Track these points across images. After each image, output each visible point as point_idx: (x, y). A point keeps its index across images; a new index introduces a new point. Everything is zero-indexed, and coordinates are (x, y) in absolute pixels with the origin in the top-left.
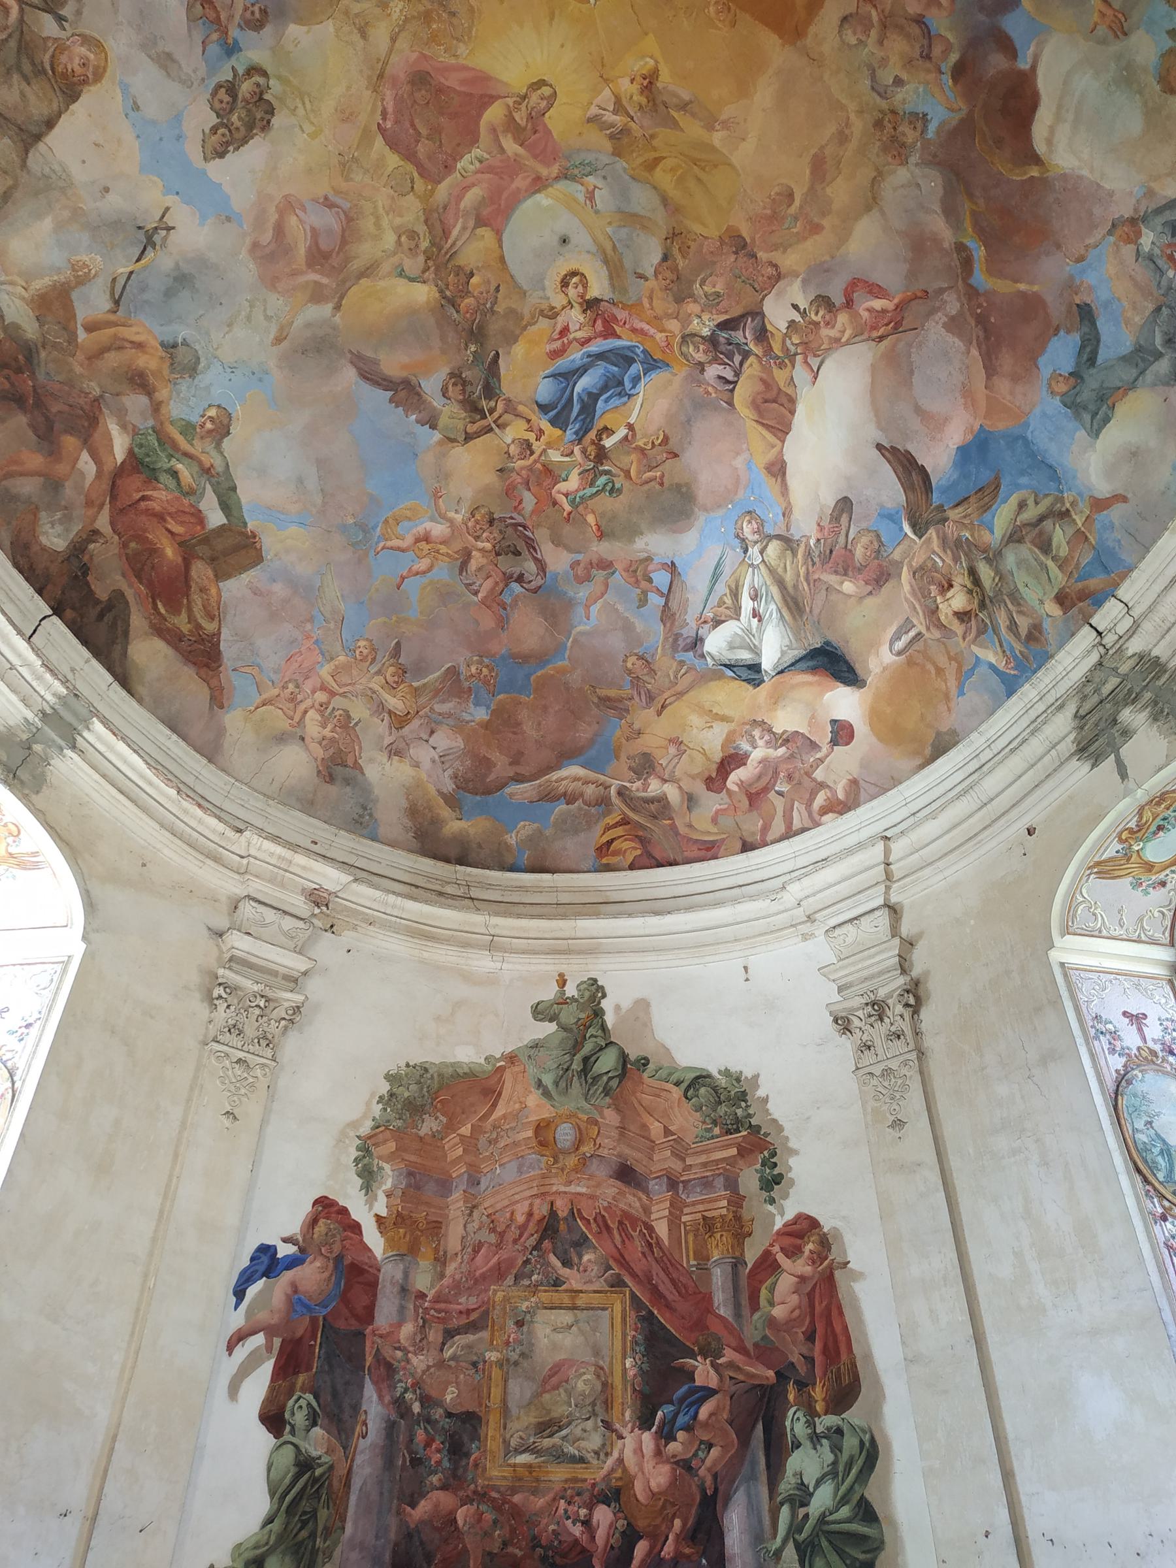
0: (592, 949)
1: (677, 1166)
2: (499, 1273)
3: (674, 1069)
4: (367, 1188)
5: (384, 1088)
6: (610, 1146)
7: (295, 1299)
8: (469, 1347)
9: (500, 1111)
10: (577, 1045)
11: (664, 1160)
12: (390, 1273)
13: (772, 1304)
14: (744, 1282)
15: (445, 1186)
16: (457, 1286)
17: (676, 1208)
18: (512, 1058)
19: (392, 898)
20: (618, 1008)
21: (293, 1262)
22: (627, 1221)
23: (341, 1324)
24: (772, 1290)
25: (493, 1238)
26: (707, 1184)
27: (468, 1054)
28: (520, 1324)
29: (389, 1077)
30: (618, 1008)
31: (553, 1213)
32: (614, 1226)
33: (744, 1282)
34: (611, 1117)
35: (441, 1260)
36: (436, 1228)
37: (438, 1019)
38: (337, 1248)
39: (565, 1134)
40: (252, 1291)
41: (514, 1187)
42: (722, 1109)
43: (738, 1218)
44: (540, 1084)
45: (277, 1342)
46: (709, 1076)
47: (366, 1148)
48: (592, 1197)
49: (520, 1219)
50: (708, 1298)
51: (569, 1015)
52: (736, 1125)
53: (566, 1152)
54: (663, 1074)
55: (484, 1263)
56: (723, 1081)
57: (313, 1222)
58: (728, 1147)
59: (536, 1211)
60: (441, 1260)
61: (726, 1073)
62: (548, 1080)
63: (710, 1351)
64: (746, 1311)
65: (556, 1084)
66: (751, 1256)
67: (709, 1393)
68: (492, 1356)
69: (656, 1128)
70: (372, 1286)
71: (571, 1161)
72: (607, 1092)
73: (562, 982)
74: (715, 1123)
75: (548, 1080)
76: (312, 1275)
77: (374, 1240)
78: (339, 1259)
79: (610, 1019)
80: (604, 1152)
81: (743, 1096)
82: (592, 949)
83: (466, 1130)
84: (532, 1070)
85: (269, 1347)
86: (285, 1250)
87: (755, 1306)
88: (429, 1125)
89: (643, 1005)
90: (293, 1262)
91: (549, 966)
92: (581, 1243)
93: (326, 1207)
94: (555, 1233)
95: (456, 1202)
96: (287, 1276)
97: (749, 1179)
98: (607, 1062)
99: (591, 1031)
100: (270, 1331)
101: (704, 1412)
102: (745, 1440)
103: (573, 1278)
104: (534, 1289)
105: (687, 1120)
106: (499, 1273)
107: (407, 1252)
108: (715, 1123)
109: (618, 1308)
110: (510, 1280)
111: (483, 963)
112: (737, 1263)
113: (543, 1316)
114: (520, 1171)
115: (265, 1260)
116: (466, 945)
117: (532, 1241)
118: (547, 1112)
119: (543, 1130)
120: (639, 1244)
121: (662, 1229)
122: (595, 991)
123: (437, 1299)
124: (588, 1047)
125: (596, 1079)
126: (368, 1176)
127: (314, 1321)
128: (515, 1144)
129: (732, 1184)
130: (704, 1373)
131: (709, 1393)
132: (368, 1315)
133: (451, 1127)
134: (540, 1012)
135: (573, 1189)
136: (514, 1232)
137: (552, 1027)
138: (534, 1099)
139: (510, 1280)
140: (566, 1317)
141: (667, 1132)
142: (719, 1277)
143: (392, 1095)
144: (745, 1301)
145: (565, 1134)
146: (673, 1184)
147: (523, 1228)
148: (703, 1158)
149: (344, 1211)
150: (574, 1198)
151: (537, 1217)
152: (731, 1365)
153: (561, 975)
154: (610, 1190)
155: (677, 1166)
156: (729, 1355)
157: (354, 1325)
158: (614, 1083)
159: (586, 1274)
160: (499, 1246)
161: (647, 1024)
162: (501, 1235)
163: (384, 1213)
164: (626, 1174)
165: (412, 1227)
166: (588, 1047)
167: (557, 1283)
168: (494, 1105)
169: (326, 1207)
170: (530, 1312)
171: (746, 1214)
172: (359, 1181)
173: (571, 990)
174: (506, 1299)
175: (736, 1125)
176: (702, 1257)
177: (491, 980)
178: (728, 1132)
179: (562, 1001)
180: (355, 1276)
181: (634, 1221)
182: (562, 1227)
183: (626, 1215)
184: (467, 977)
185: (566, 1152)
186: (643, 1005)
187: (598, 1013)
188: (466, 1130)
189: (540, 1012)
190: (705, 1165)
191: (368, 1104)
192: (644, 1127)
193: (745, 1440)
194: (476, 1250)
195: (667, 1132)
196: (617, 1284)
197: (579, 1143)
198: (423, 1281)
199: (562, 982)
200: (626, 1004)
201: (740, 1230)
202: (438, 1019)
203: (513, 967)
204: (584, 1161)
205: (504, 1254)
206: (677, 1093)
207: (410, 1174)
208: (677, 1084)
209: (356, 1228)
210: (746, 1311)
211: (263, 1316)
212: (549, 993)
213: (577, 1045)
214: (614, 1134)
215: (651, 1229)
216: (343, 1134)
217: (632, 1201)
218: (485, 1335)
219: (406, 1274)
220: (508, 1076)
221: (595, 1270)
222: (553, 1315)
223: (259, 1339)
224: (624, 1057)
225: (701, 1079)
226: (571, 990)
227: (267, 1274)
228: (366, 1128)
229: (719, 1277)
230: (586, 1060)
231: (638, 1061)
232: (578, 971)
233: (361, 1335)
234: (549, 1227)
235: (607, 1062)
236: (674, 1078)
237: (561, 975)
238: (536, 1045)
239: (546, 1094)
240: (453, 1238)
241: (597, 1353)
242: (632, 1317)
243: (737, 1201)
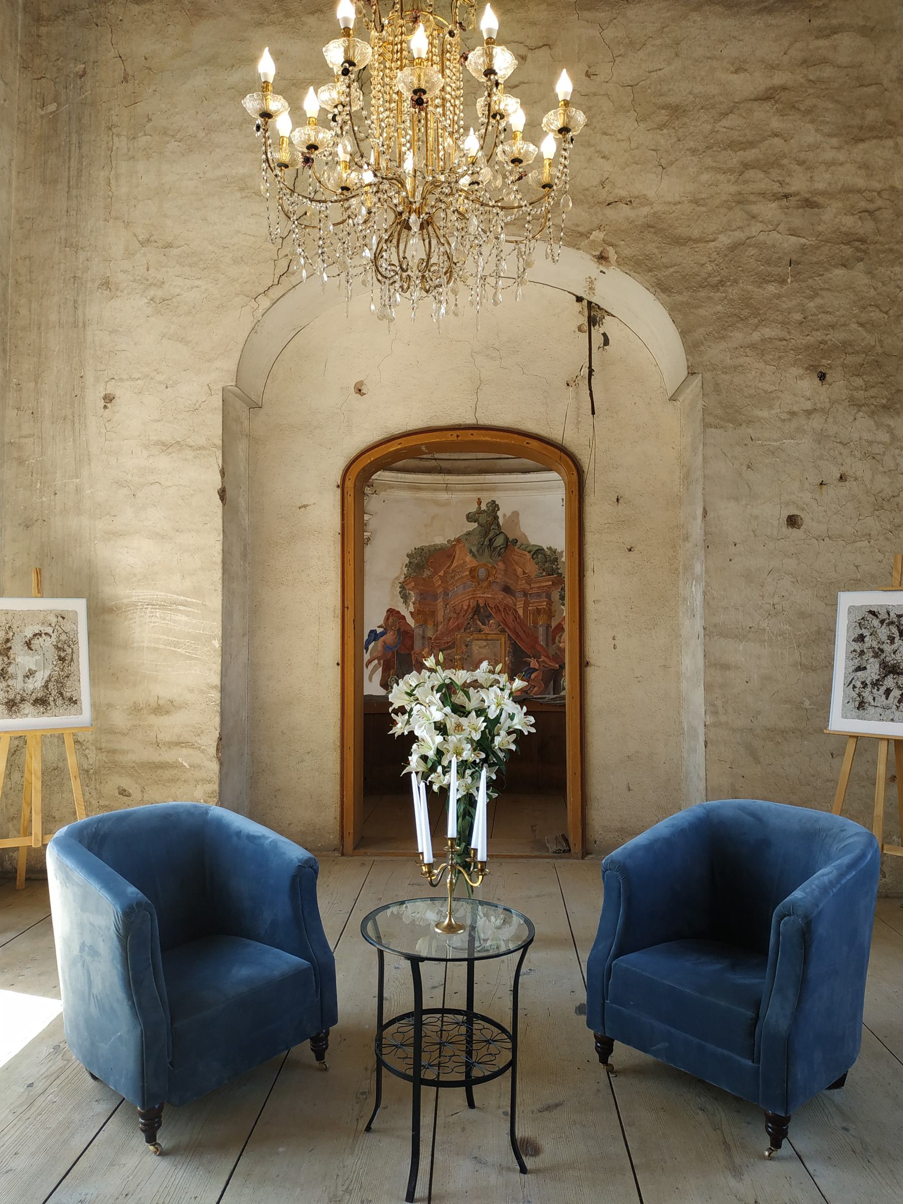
0: (493, 488)
1: (528, 587)
2: (458, 628)
3: (528, 545)
4: (405, 602)
5: (407, 560)
6: (500, 577)
7: (386, 647)
8: (449, 654)
9: (455, 564)
10: (486, 534)
11: (522, 584)
12: (418, 632)
13: (560, 642)
14: (550, 634)
15: (435, 597)
16: (442, 633)
17: (526, 604)
18: (458, 540)
19: (400, 475)
20: (504, 515)
21: (383, 634)
22: (507, 608)
23: (403, 652)
24: (560, 637)
25: (455, 615)
26: (539, 595)
27: (440, 540)
28: (467, 646)
29: (408, 556)
30: (504, 515)
31: (478, 605)
32: (502, 610)
33: (550, 634)
34: (501, 566)
35: (436, 625)
36: (433, 613)
37: (426, 525)
38: (397, 627)
39: (482, 573)
40: (370, 647)
41: (462, 596)
42: (547, 565)
43: (550, 610)
44: (471, 551)
45: (382, 661)
46: (543, 549)
47: (402, 587)
48: (494, 598)
49: (465, 608)
50: (536, 639)
51: (483, 519)
52: (551, 572)
53: (483, 581)
54: (523, 547)
55: (452, 624)
56: (548, 552)
57: (387, 618)
58: (548, 581)
59: (472, 606)
60: (436, 625)
61: (550, 549)
62: (474, 549)
63: (536, 657)
64: (550, 644)
65: (478, 551)
66: (554, 624)
67: (535, 670)
68: (457, 657)
69: (519, 571)
70: (412, 637)
71: (485, 584)
72: (499, 555)
73: (479, 503)
74: (544, 570)
75: (474, 549)
76: (390, 637)
77: (411, 621)
78: (399, 629)
79: (501, 520)
80: (498, 580)
81: (556, 560)
82: (493, 488)
83: (442, 573)
84: (467, 545)
85: (379, 664)
86: (379, 630)
87: (554, 643)
88: (427, 573)
89: (516, 514)
90: (383, 634)
91: (474, 496)
92: (489, 616)
93: (391, 612)
94: (480, 613)
95: (440, 603)
96: (382, 638)
97: (556, 595)
98: (499, 541)
99: (493, 527)
100: (379, 658)
101: (533, 676)
102: (546, 686)
103: (486, 629)
104: (471, 633)
105: (532, 568)
106: (458, 628)
107: (423, 624)
108: (544, 570)
109: (503, 640)
110: (462, 630)
111: (443, 496)
112: (549, 626)
113: (475, 642)
114: (464, 589)
115: (373, 635)
116: (435, 490)
117: (470, 616)
118: (475, 563)
119: (472, 571)
120: (512, 617)
121: (521, 612)
122: (494, 507)
123: (436, 639)
124: (491, 535)
125: (495, 548)
126: (405, 598)
127: (393, 652)
128: (462, 578)
129: (549, 596)
130: (534, 663)
131: (535, 670)
132: (412, 647)
133: (436, 573)
134: (470, 518)
135: (485, 595)
136: (463, 613)
137: (476, 525)
138: (469, 558)
139: (462, 630)
140: (484, 643)
141: (524, 573)
142: (541, 630)
143: (410, 563)
144: (550, 641)
145: (482, 573)
146: (525, 595)
147: (466, 611)
148: (538, 585)
149: (398, 612)
150: (486, 599)
151: (472, 606)
152: (543, 661)
153: (479, 499)
154: (501, 595)
155: (528, 587)
156: (543, 658)
157: (407, 652)
158: (503, 550)
159: (490, 628)
160: (457, 618)
161: (517, 524)
162: (458, 614)
163: (413, 610)
164: (507, 589)
165: (423, 614)
166: (491, 535)
167: (480, 631)
168: (452, 562)
169: (391, 612)
170: (471, 641)
171: (553, 610)
172: (402, 600)
173: (484, 507)
174: (461, 637)
175: (551, 572)
176: (535, 623)
177: (447, 504)
178: (549, 575)
179: (480, 512)
180: (405, 634)
181: (510, 608)
182: (482, 610)
183: (507, 605)
184: (437, 503)
185: (483, 581)
186: (516, 514)
187: (496, 518)
188: (442, 573)
189: (470, 518)
190: (538, 588)
191: (402, 569)
192: (515, 570)
193: (546, 686)
194: (449, 621)
195: (524, 573)
196: (503, 631)
197: (488, 576)
198: (430, 633)
199: (479, 503)
200: (508, 514)
201: (550, 614)
202: (426, 525)
203: (456, 497)
204: (490, 584)
205: (460, 621)
206: (529, 556)
207: (421, 594)
208: (529, 552)
209: (404, 618)
210: (550, 644)
211: (375, 654)
212: (473, 508)
213: (486, 534)
214: (502, 573)
215: (516, 612)
216: (393, 582)
217: (509, 600)
218: (454, 650)
219: (424, 632)
220: (457, 549)
221: (494, 626)
222: (479, 642)
223: (376, 662)
224: (507, 539)
225: (540, 550)
226: (484, 507)
227: (374, 640)
228: (402, 580)
229: (541, 630)
230: (490, 540)
231: (513, 540)
232: (486, 497)
233: (410, 655)
234: (477, 610)
235: (499, 541)
236: (528, 549)
237: (479, 499)
238: (469, 534)
239: (474, 556)
240: (440, 617)
241: (495, 655)
242: (508, 643)
243: (550, 603)
